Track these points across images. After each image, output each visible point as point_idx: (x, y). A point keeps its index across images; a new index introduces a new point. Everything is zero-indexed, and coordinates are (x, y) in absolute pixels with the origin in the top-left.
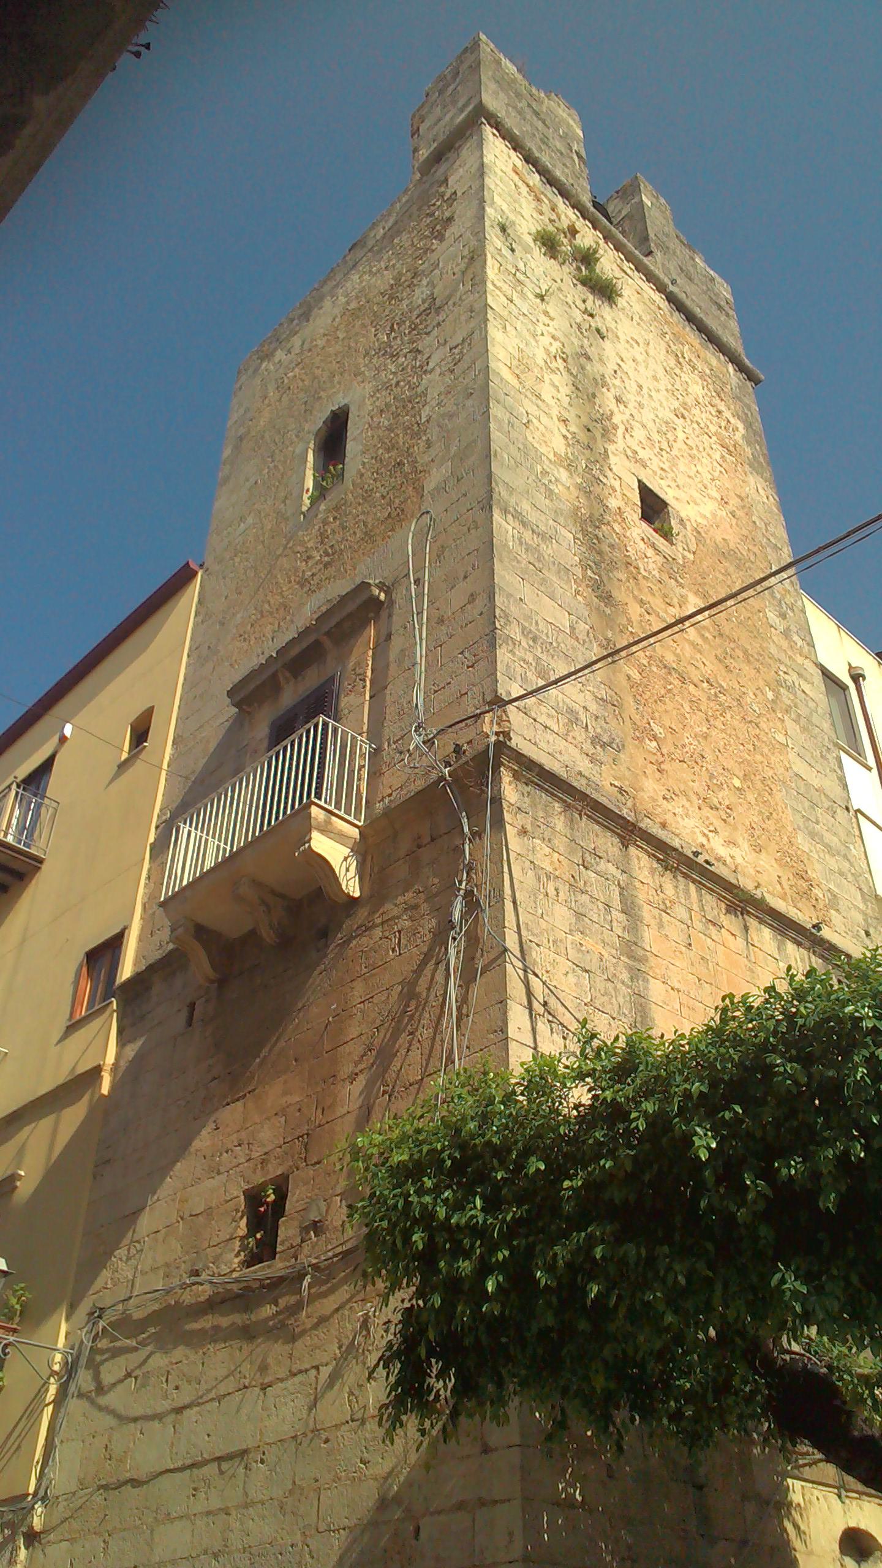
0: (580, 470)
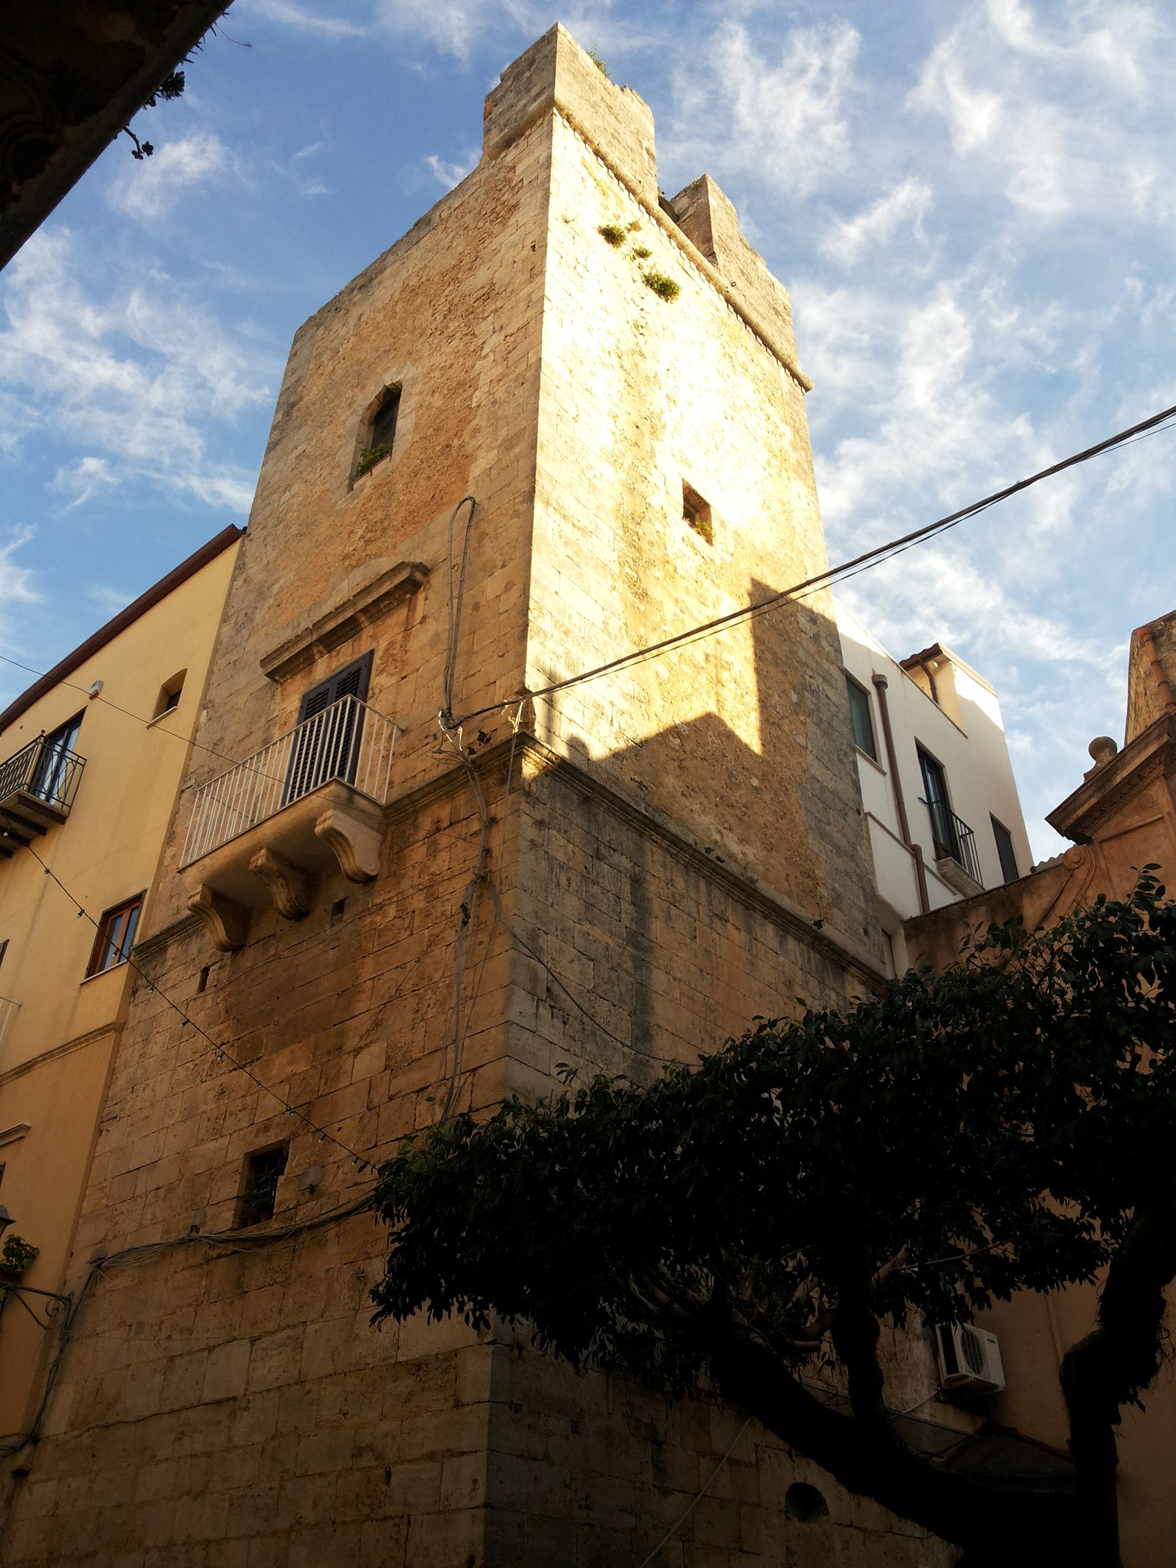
0: (626, 466)
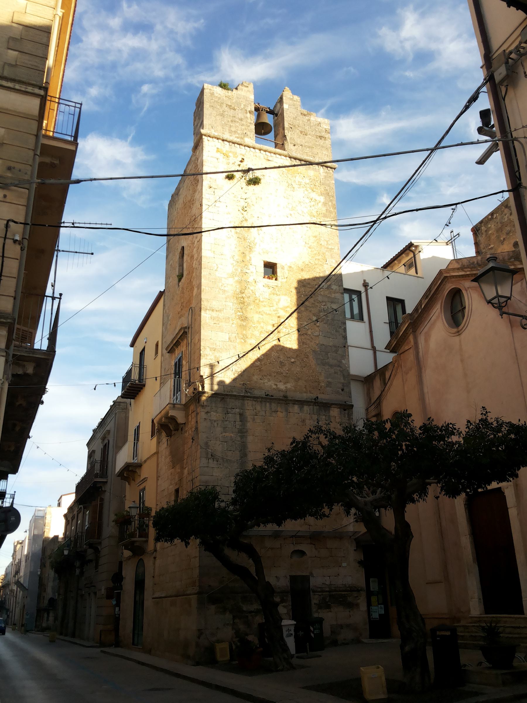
0: (238, 273)
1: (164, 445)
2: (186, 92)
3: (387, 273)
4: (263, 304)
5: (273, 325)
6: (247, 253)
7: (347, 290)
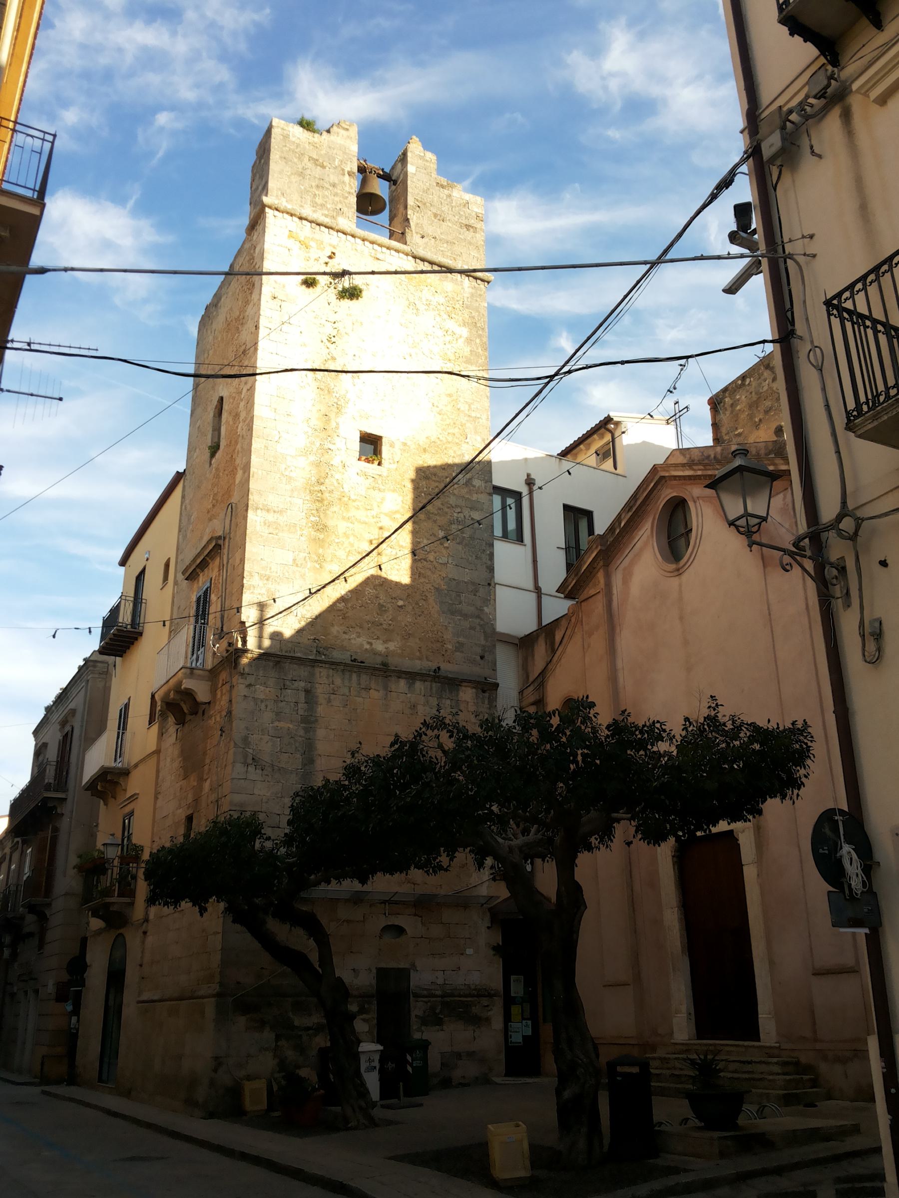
0: (315, 450)
1: (171, 737)
2: (232, 131)
3: (566, 464)
4: (355, 504)
5: (371, 542)
6: (332, 415)
7: (498, 490)
